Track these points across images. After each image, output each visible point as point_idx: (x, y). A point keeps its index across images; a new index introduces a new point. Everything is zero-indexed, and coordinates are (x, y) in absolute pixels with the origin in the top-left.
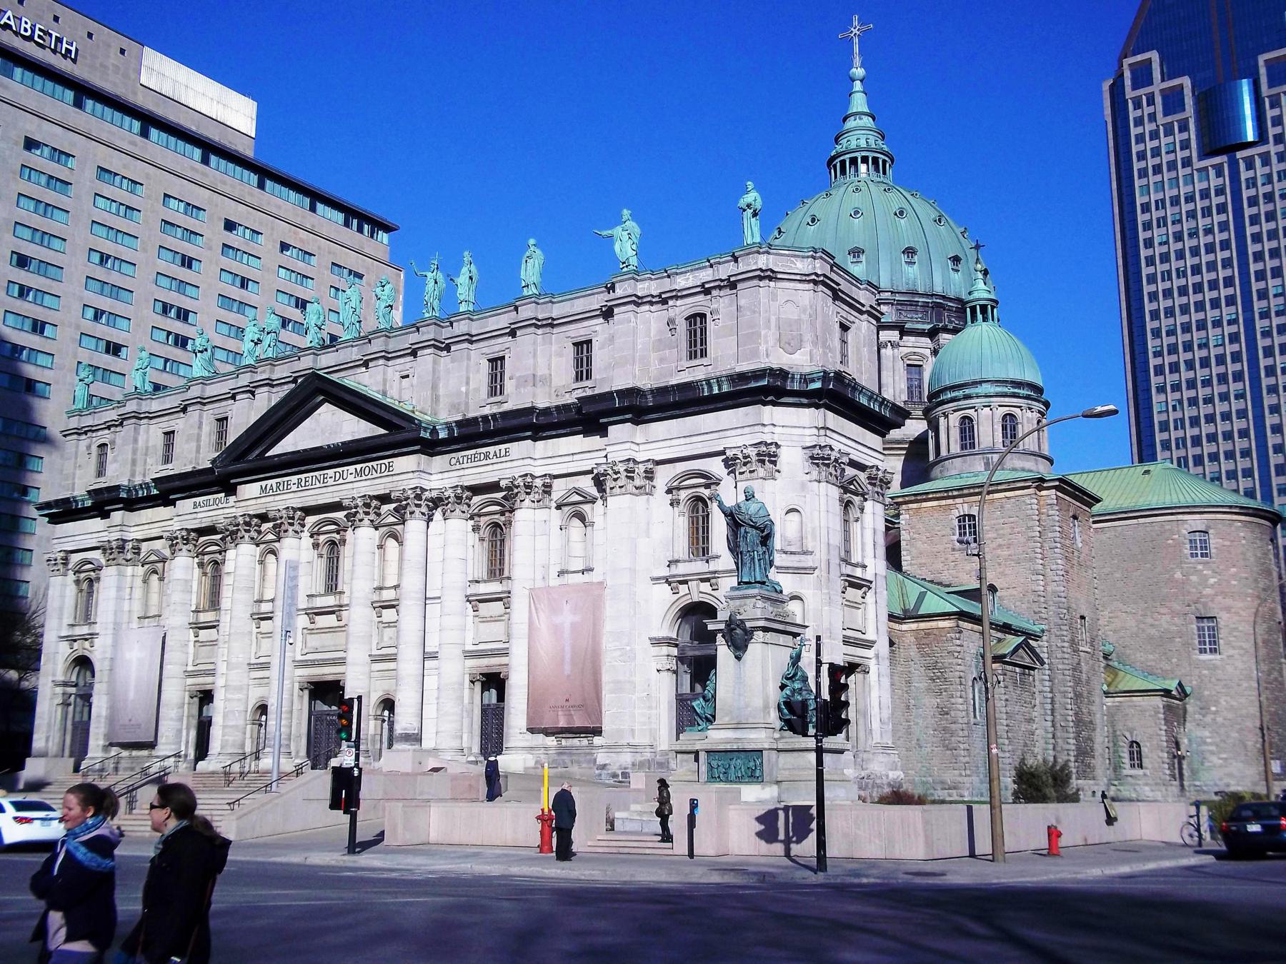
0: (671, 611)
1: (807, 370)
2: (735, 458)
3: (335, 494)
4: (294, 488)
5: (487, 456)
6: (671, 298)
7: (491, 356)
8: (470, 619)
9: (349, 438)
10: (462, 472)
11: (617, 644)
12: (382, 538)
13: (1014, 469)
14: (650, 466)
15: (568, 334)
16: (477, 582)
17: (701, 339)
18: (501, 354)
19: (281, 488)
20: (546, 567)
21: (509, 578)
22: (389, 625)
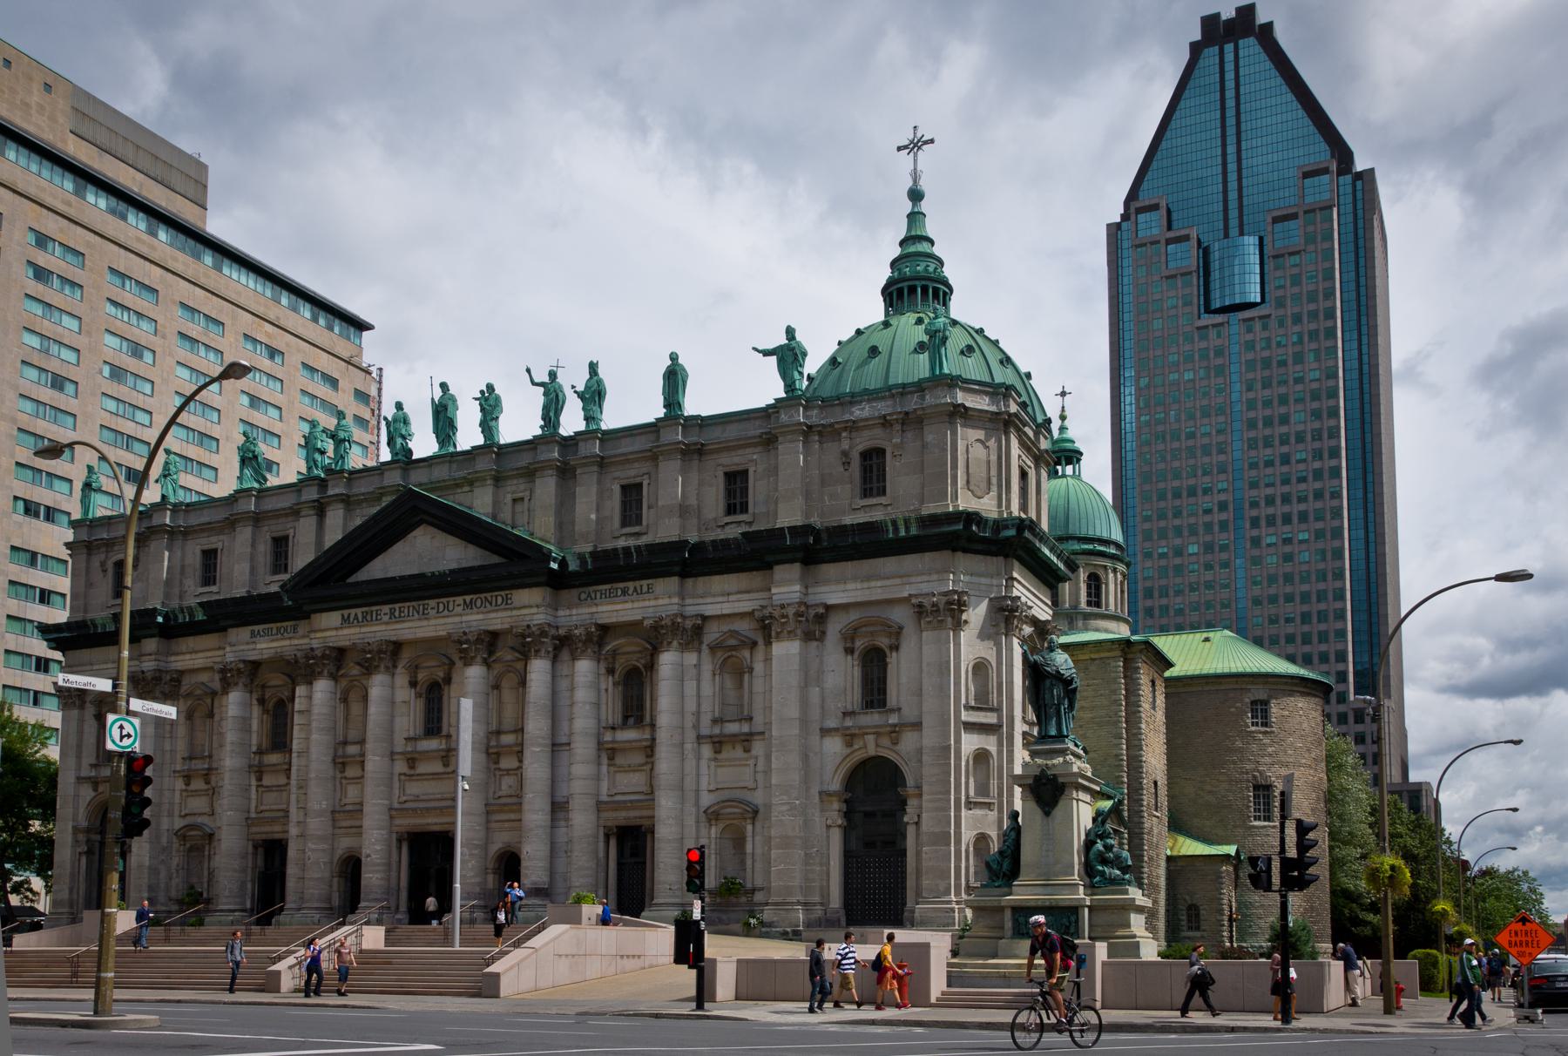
0: (842, 766)
1: (995, 515)
2: (920, 606)
3: (439, 628)
5: (625, 592)
6: (845, 429)
7: (625, 482)
8: (604, 768)
9: (454, 566)
10: (594, 609)
11: (785, 797)
12: (499, 678)
13: (1097, 630)
14: (821, 610)
15: (720, 461)
16: (613, 728)
17: (878, 476)
18: (638, 480)
19: (369, 618)
20: (698, 714)
21: (653, 726)
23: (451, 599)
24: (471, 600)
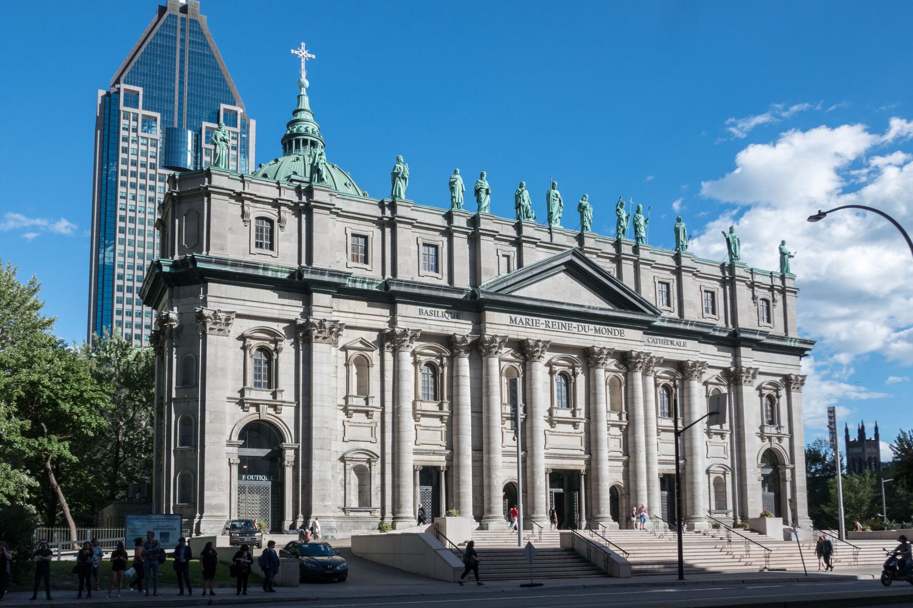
3: (580, 340)
4: (543, 327)
5: (672, 343)
18: (667, 281)
19: (530, 322)
22: (615, 437)
23: (587, 325)
24: (599, 328)
